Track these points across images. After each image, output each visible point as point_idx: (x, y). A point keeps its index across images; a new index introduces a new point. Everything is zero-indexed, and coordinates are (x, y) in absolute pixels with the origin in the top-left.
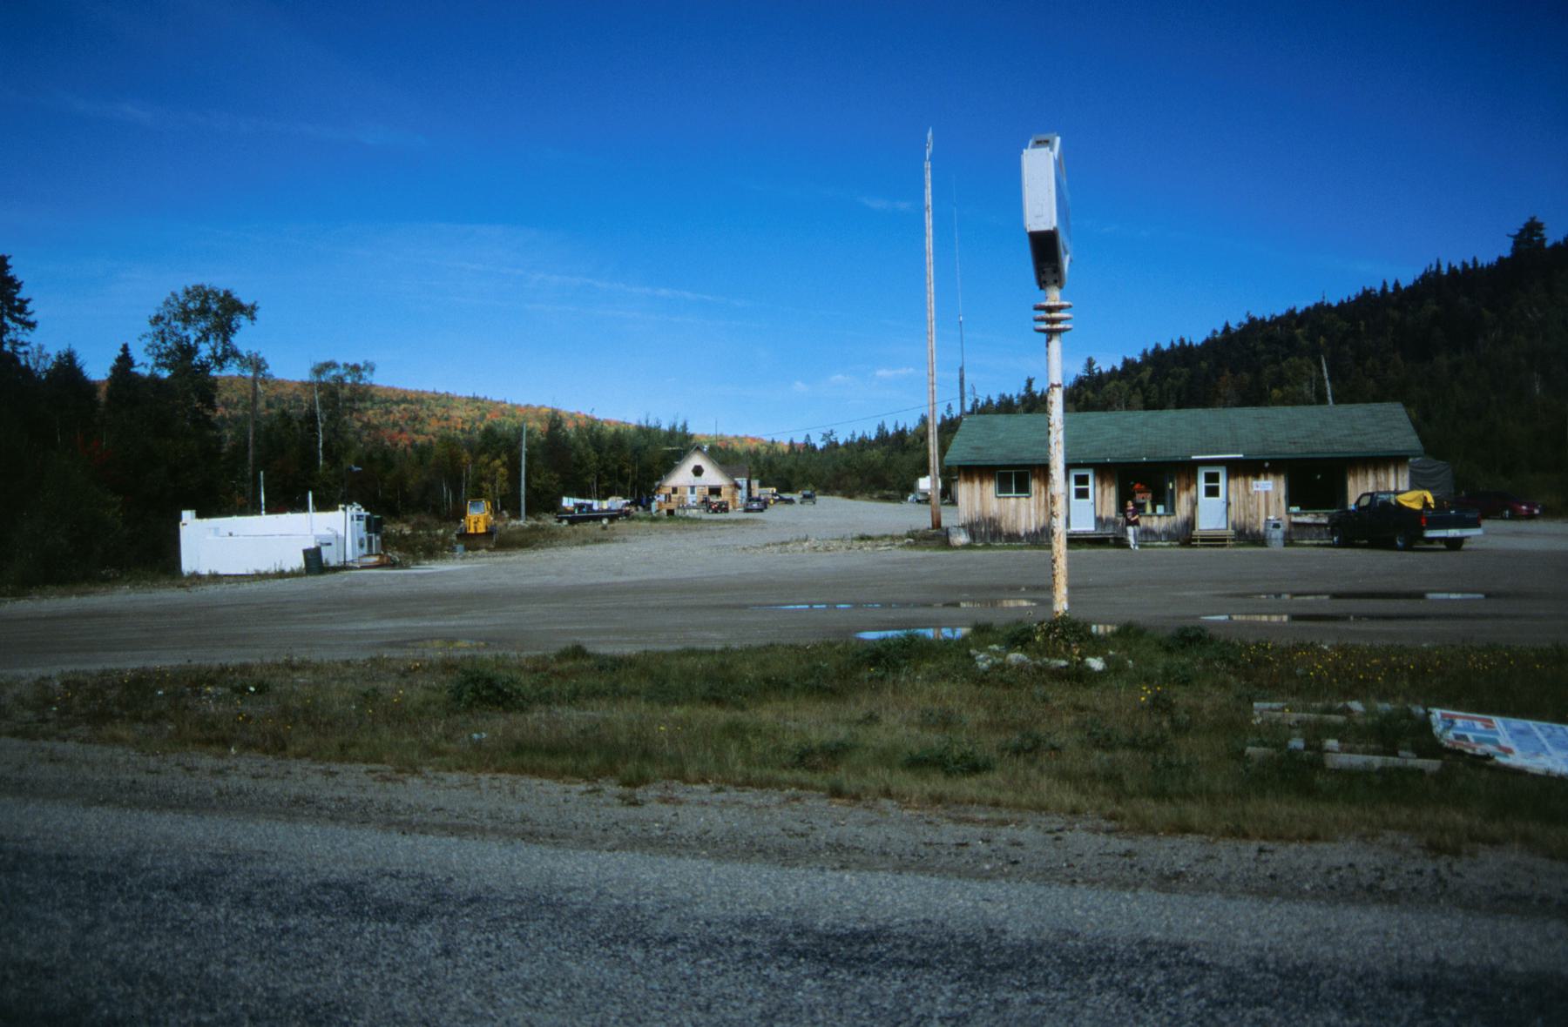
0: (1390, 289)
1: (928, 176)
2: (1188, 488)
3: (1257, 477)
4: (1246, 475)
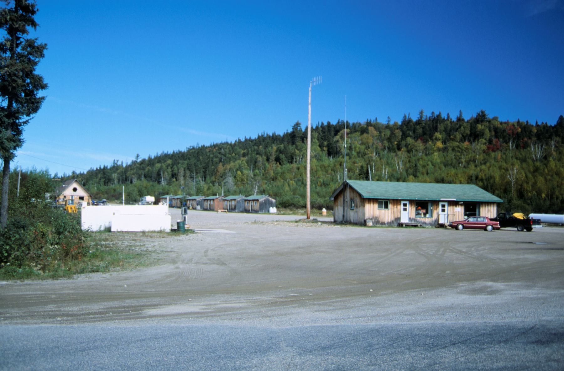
0: (428, 119)
1: (310, 93)
2: (436, 209)
3: (456, 206)
4: (453, 205)
